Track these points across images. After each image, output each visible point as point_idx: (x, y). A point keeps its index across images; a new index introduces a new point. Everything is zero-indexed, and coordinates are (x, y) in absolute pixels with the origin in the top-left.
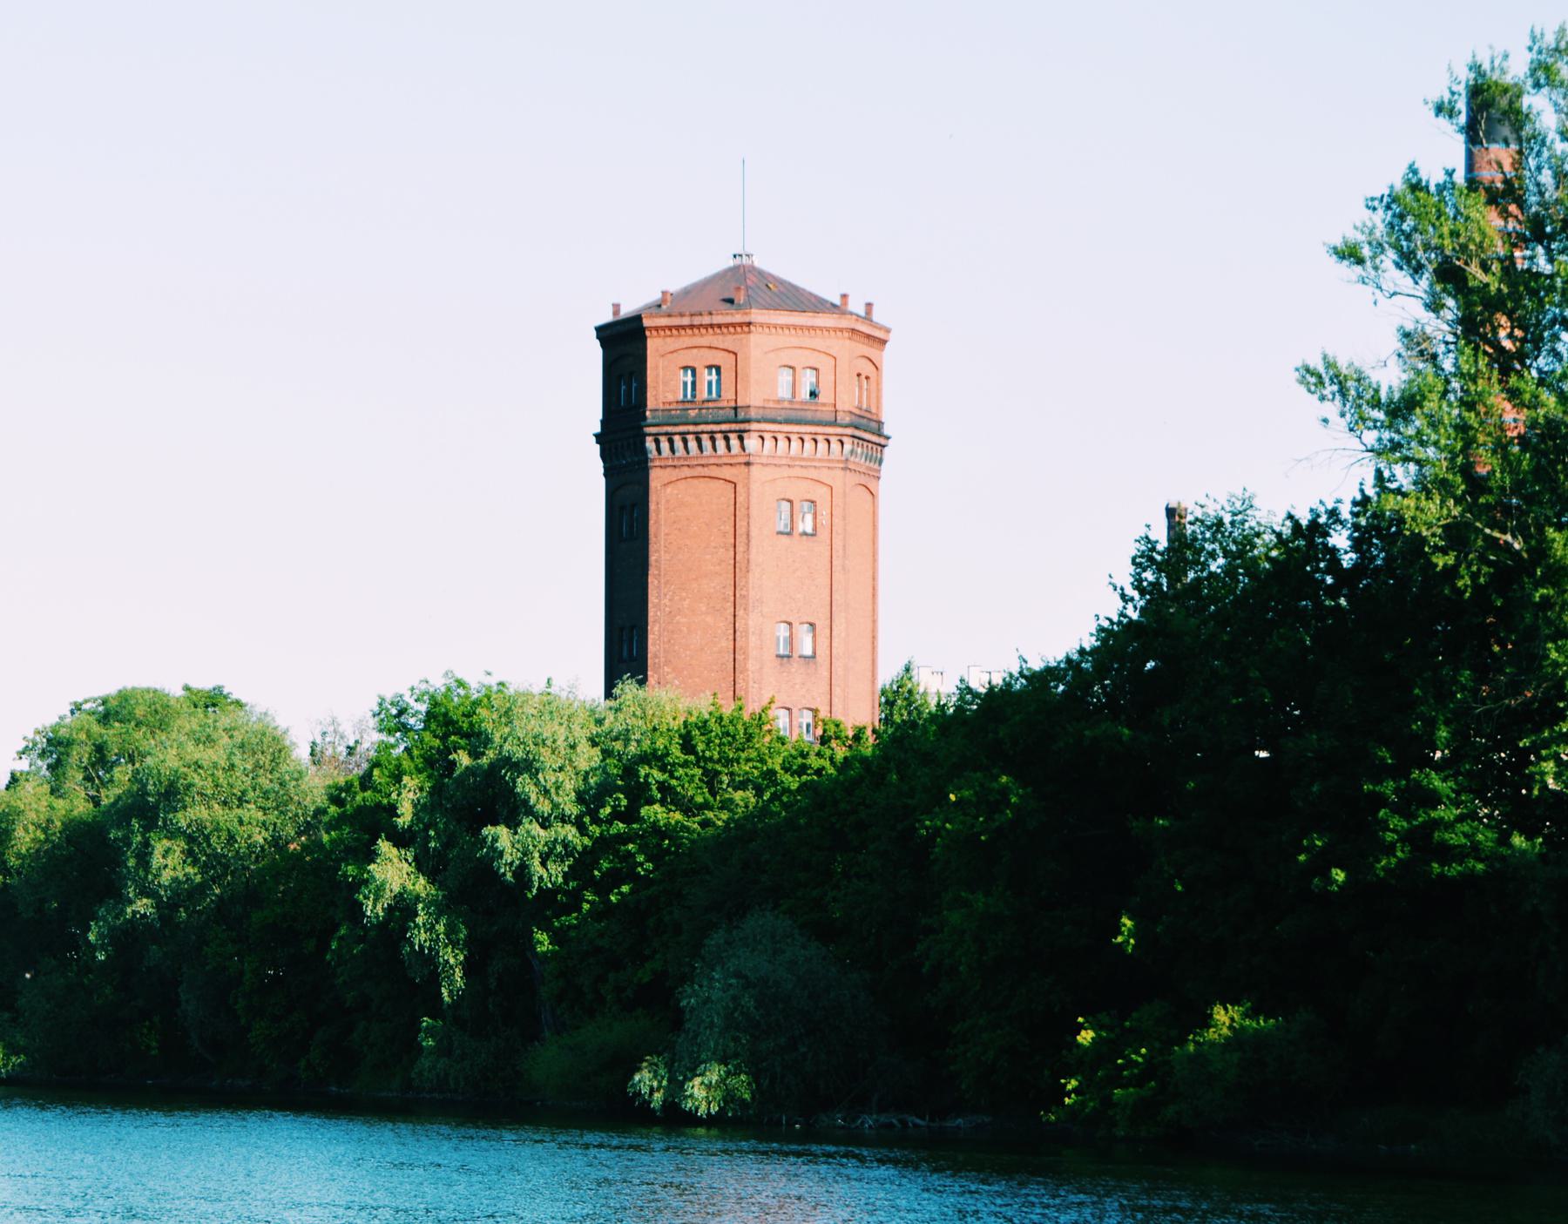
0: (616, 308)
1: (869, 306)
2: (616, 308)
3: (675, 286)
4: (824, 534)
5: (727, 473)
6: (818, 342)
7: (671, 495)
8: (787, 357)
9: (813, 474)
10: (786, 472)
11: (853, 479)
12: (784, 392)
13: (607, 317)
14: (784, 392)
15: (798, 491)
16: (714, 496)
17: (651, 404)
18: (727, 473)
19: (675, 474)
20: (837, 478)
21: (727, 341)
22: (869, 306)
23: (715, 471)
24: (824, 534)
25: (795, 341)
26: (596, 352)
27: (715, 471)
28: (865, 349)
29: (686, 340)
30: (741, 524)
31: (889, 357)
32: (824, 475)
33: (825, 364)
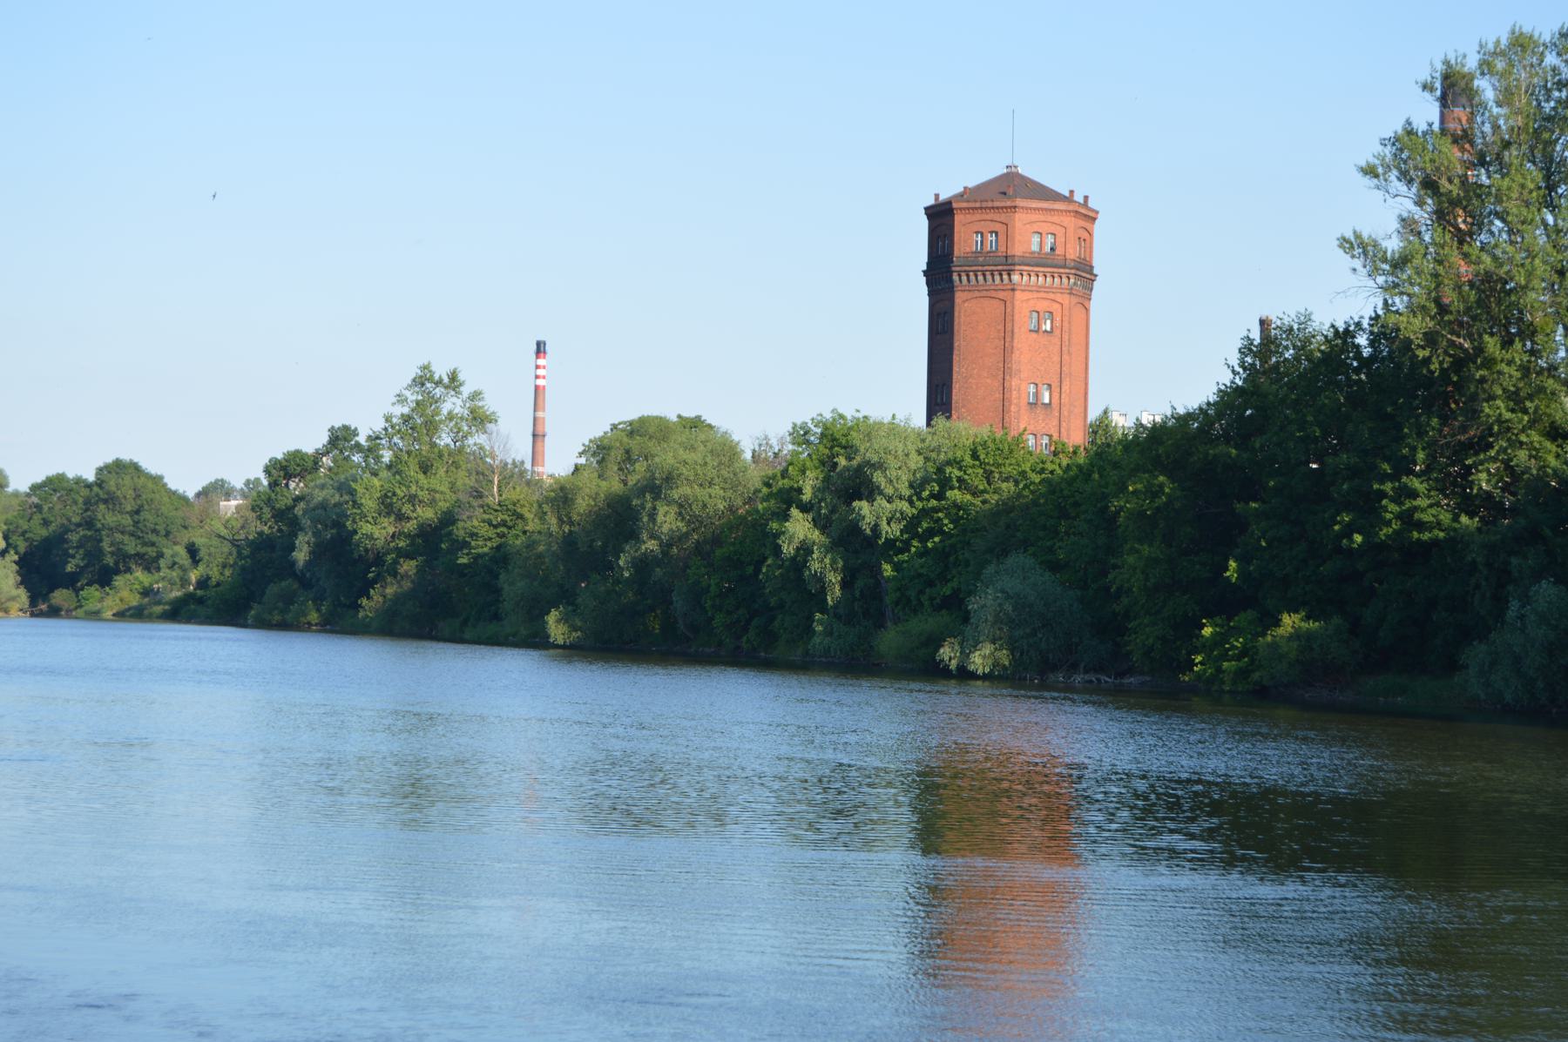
0: (937, 196)
1: (1086, 198)
2: (937, 196)
3: (971, 185)
4: (1057, 333)
5: (1001, 295)
6: (1055, 219)
7: (967, 307)
8: (1036, 227)
9: (1051, 296)
10: (1036, 295)
11: (1074, 300)
12: (1035, 248)
13: (931, 202)
14: (1035, 248)
15: (1043, 306)
16: (992, 308)
17: (956, 253)
18: (1001, 295)
19: (970, 295)
20: (1065, 299)
21: (1003, 217)
22: (1086, 198)
23: (994, 294)
24: (1057, 333)
25: (1042, 218)
26: (924, 223)
27: (994, 294)
28: (1082, 223)
29: (978, 216)
30: (1009, 325)
31: (1098, 228)
32: (1059, 297)
33: (1060, 231)
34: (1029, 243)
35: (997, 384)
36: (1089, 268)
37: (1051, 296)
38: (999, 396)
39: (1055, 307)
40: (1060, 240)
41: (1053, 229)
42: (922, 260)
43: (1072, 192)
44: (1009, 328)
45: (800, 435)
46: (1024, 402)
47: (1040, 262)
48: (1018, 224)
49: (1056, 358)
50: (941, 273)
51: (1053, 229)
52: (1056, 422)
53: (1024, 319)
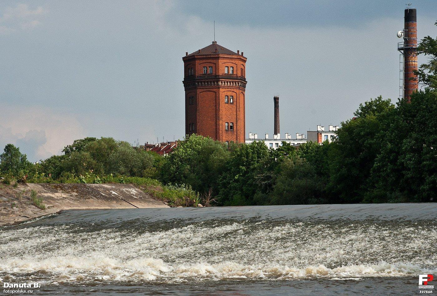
0: (187, 53)
1: (242, 53)
2: (187, 53)
3: (200, 49)
4: (235, 103)
5: (214, 90)
6: (233, 61)
8: (226, 65)
9: (233, 90)
10: (227, 90)
11: (240, 91)
12: (226, 72)
13: (185, 55)
14: (226, 72)
15: (229, 94)
16: (211, 95)
17: (197, 75)
18: (214, 90)
19: (202, 90)
20: (237, 91)
21: (214, 61)
22: (242, 53)
23: (211, 90)
24: (235, 103)
25: (228, 61)
26: (182, 63)
27: (211, 90)
28: (242, 63)
29: (204, 61)
30: (217, 101)
31: (247, 64)
32: (235, 90)
33: (235, 66)
34: (224, 70)
35: (214, 123)
36: (244, 79)
37: (233, 90)
38: (214, 127)
39: (235, 66)
40: (235, 69)
41: (232, 65)
42: (181, 76)
43: (238, 51)
44: (217, 102)
45: (109, 138)
46: (224, 130)
47: (228, 77)
48: (220, 63)
49: (235, 113)
50: (191, 82)
51: (232, 65)
52: (235, 137)
53: (223, 100)
